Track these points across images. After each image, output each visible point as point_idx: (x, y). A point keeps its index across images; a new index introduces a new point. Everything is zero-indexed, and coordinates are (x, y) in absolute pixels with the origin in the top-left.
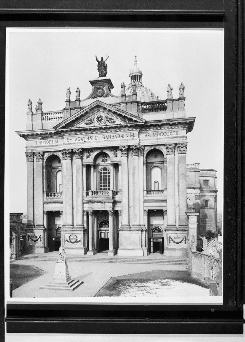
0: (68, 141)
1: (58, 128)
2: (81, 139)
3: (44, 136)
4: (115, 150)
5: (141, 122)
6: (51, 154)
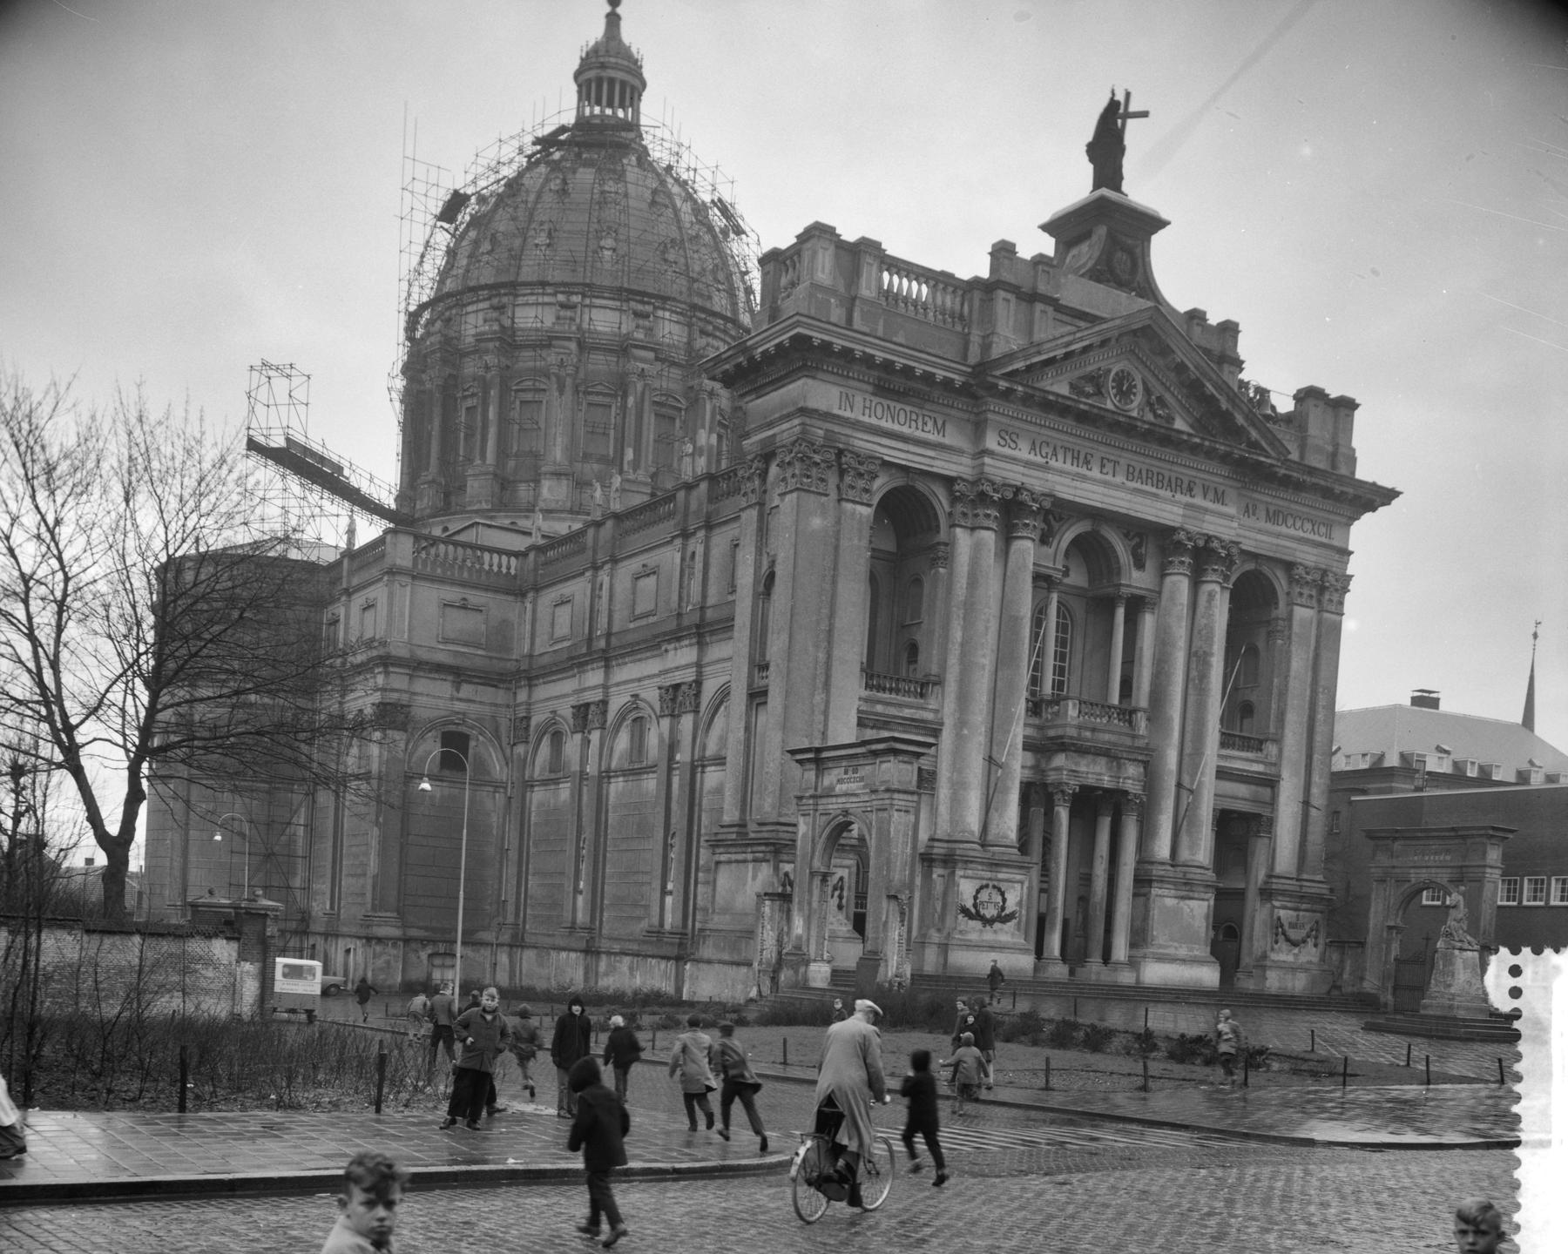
0: (1003, 442)
1: (998, 373)
2: (1050, 451)
4: (1137, 540)
5: (1273, 453)
6: (899, 481)
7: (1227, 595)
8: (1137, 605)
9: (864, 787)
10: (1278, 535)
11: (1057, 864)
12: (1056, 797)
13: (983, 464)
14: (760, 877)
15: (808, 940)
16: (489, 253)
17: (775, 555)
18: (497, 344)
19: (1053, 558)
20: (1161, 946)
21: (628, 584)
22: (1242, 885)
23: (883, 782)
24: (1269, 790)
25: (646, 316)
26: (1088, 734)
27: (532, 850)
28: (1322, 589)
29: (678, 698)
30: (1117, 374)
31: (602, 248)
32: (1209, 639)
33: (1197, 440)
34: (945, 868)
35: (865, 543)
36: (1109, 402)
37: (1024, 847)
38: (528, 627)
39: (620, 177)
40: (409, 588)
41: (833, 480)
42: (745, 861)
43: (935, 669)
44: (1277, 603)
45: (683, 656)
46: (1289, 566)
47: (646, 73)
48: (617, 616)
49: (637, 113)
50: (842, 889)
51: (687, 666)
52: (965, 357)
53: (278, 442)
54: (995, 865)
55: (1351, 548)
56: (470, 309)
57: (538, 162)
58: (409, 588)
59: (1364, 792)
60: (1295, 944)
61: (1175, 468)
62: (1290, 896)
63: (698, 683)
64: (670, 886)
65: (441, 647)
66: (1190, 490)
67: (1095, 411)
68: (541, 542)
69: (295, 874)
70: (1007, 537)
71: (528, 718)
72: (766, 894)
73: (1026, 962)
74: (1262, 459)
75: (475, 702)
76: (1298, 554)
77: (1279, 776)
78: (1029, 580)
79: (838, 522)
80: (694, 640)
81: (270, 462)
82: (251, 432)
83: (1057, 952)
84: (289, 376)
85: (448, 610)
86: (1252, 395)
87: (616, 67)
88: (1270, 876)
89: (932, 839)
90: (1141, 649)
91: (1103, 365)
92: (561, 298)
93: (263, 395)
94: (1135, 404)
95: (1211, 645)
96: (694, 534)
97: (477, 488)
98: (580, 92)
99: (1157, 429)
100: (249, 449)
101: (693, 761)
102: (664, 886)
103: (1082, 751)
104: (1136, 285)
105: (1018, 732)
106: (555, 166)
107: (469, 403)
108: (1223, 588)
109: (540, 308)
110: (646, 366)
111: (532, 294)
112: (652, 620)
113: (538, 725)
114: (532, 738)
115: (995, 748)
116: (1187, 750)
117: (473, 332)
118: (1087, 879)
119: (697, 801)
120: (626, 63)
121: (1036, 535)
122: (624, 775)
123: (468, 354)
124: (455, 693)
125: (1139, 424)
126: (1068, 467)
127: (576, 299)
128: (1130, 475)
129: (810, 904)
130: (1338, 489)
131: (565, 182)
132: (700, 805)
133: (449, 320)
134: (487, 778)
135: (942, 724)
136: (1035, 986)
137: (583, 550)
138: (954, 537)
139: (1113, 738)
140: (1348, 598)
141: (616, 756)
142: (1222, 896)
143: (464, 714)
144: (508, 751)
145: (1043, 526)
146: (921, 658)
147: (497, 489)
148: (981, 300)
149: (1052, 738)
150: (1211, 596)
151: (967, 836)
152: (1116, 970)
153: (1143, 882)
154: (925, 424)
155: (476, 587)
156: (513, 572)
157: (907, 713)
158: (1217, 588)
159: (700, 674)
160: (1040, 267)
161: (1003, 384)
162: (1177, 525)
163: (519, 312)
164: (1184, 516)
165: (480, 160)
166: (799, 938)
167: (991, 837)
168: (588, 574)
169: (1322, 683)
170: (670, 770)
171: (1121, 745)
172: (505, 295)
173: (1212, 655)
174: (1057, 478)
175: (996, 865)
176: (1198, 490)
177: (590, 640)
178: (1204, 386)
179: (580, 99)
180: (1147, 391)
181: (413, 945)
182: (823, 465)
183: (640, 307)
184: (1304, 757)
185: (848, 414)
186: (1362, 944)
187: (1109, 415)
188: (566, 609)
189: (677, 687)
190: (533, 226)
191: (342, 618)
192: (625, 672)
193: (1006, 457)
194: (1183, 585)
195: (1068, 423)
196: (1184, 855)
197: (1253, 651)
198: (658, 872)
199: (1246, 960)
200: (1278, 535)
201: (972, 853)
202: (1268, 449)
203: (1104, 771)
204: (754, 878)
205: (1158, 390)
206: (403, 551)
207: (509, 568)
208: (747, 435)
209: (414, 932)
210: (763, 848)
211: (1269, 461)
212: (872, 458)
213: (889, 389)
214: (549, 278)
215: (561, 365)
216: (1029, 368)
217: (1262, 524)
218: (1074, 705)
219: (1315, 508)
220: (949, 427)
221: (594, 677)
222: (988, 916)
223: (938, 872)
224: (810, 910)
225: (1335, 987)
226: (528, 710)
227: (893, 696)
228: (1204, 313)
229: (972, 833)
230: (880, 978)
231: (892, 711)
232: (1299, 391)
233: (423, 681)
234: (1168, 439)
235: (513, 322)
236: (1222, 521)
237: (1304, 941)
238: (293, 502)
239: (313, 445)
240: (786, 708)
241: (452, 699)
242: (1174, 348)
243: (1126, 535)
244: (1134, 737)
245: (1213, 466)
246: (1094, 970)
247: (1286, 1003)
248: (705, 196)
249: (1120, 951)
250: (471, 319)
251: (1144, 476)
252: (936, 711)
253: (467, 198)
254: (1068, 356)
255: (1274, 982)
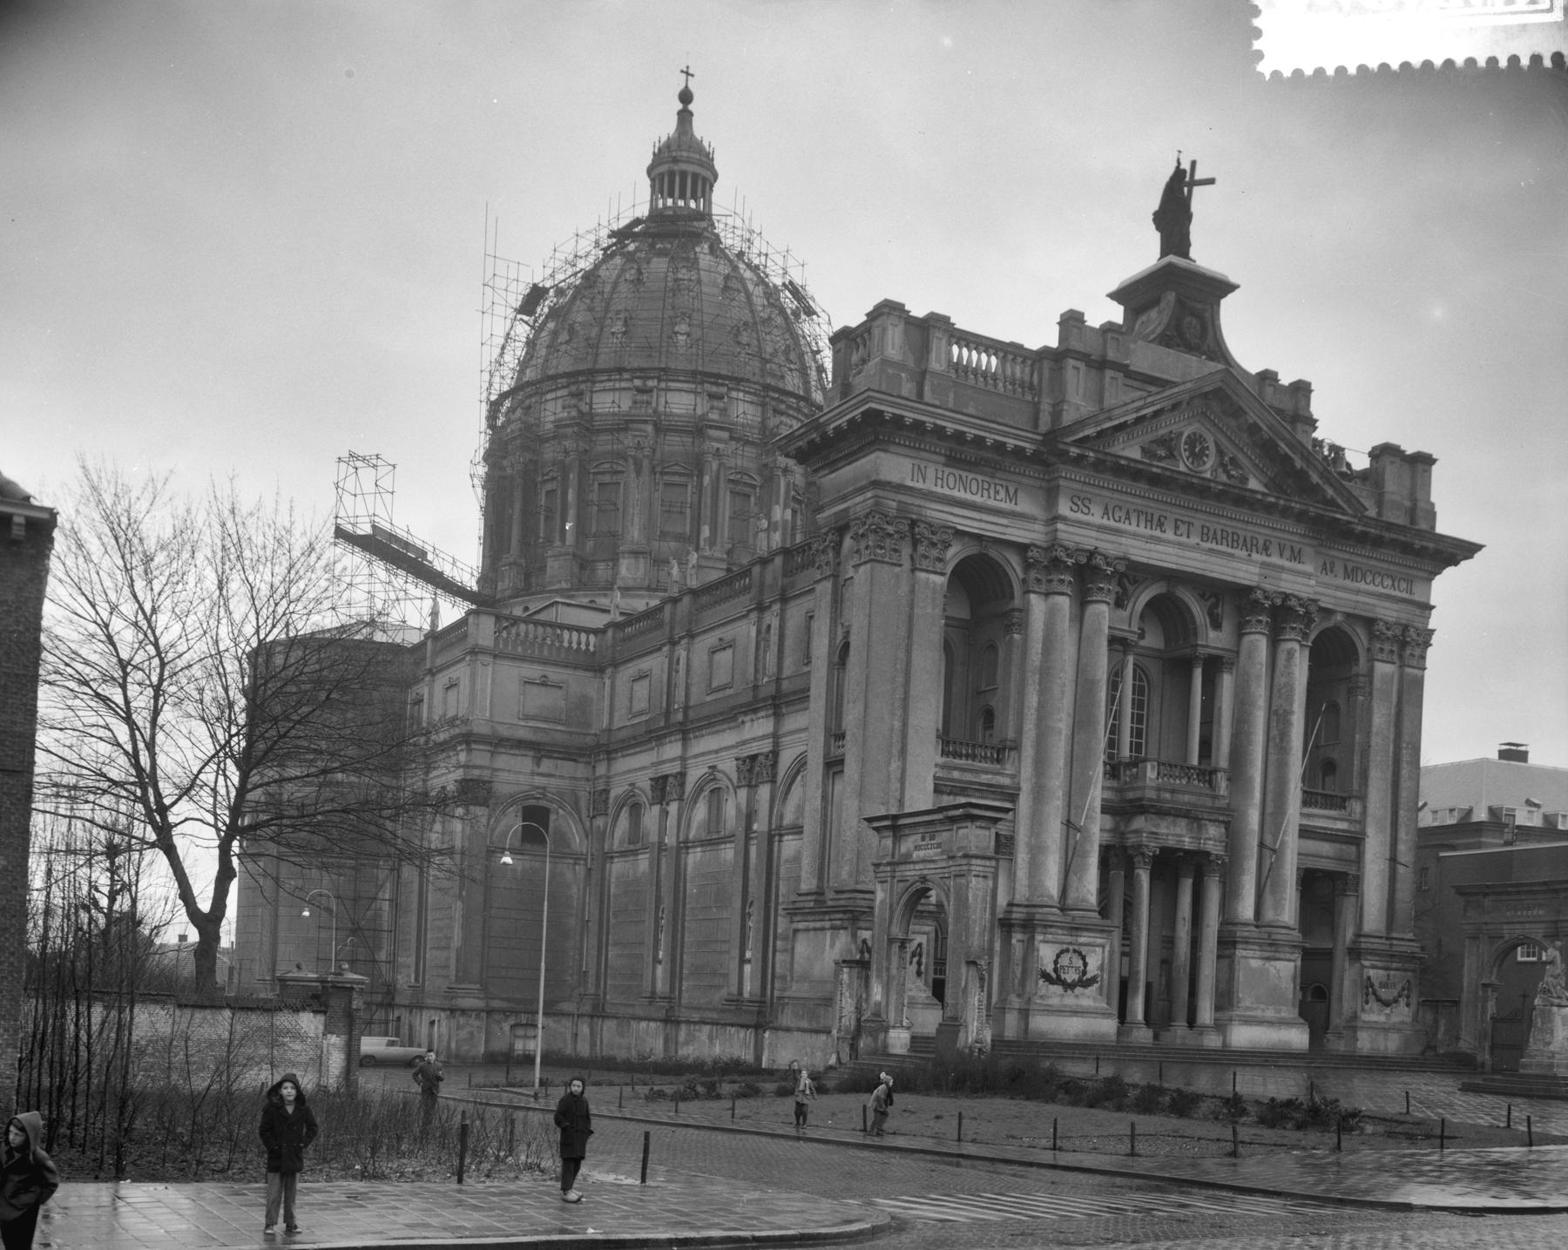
0: (1075, 508)
3: (971, 453)
4: (1213, 600)
5: (1350, 512)
6: (972, 549)
7: (1307, 652)
8: (1214, 666)
9: (942, 853)
10: (1358, 592)
11: (1139, 929)
12: (1136, 860)
13: (1056, 530)
14: (838, 945)
15: (887, 1005)
16: (567, 342)
17: (849, 626)
18: (576, 429)
19: (1128, 621)
20: (1247, 1009)
21: (706, 657)
22: (1330, 946)
23: (959, 849)
24: (1353, 848)
25: (720, 397)
26: (1167, 796)
27: (612, 921)
28: (1403, 644)
29: (756, 769)
30: (1189, 437)
31: (676, 333)
32: (1290, 699)
33: (1273, 500)
34: (1024, 933)
35: (938, 611)
36: (1181, 464)
37: (1104, 911)
38: (607, 703)
39: (694, 264)
40: (490, 668)
41: (906, 551)
42: (823, 929)
43: (1011, 735)
44: (1357, 660)
45: (762, 726)
46: (1369, 623)
47: (718, 165)
48: (694, 690)
49: (708, 203)
50: (920, 955)
51: (764, 737)
52: (1036, 425)
53: (365, 529)
54: (1075, 929)
55: (1432, 603)
56: (549, 396)
57: (613, 255)
58: (490, 668)
59: (1453, 848)
60: (1386, 1004)
61: (1250, 527)
62: (1379, 955)
63: (775, 753)
64: (748, 955)
65: (522, 723)
66: (1266, 548)
67: (1168, 473)
68: (620, 619)
69: (381, 948)
70: (1082, 601)
71: (607, 791)
72: (844, 961)
73: (1109, 1026)
74: (1338, 516)
75: (557, 776)
76: (1378, 610)
77: (1364, 834)
78: (1105, 643)
79: (912, 591)
80: (771, 712)
81: (357, 549)
82: (339, 521)
83: (1140, 1016)
84: (375, 466)
85: (528, 686)
86: (1326, 453)
87: (688, 161)
88: (1358, 935)
89: (1011, 904)
90: (1220, 708)
91: (1175, 428)
92: (638, 382)
93: (350, 485)
94: (1208, 465)
95: (1291, 704)
96: (770, 607)
97: (556, 568)
98: (653, 186)
99: (1232, 490)
100: (336, 537)
101: (770, 830)
102: (742, 954)
103: (1162, 812)
104: (1205, 348)
105: (1097, 793)
106: (630, 257)
107: (549, 487)
108: (1302, 646)
109: (617, 394)
110: (721, 446)
111: (610, 380)
112: (729, 692)
113: (617, 798)
114: (611, 811)
115: (1073, 812)
116: (1269, 810)
117: (552, 418)
118: (1170, 942)
119: (774, 870)
120: (698, 156)
121: (1111, 599)
122: (702, 846)
123: (547, 440)
124: (536, 769)
125: (1212, 485)
126: (1142, 530)
127: (651, 383)
128: (1205, 535)
129: (888, 969)
130: (1418, 543)
131: (639, 272)
132: (778, 874)
133: (529, 407)
134: (567, 851)
135: (1019, 789)
136: (1119, 1050)
137: (660, 625)
138: (1029, 602)
139: (1193, 799)
140: (1431, 653)
141: (694, 825)
142: (1308, 955)
143: (544, 788)
144: (588, 824)
145: (1118, 589)
146: (997, 723)
147: (576, 570)
148: (1052, 369)
149: (1131, 801)
150: (1290, 654)
151: (1046, 901)
152: (1201, 1034)
153: (1227, 943)
154: (997, 492)
155: (556, 664)
156: (591, 648)
157: (984, 778)
158: (1296, 646)
159: (776, 744)
160: (1110, 335)
161: (1074, 451)
162: (1254, 584)
163: (597, 398)
164: (1260, 575)
165: (557, 254)
166: (878, 1004)
167: (1070, 902)
168: (665, 649)
169: (1406, 738)
170: (748, 839)
171: (1201, 806)
172: (583, 382)
173: (1292, 713)
174: (1131, 542)
175: (1077, 929)
176: (1274, 549)
177: (668, 713)
178: (1277, 445)
179: (653, 193)
180: (1221, 453)
181: (497, 1017)
182: (896, 536)
183: (714, 389)
184: (1389, 816)
185: (920, 485)
186: (1456, 1003)
187: (1182, 477)
188: (645, 683)
189: (753, 758)
190: (609, 315)
191: (426, 697)
192: (706, 743)
193: (1079, 522)
194: (1262, 644)
195: (1140, 487)
196: (1269, 915)
197: (1334, 708)
198: (737, 943)
199: (1336, 1020)
200: (1358, 592)
201: (1052, 918)
202: (1345, 506)
203: (1184, 832)
204: (832, 945)
205: (1231, 451)
206: (485, 631)
207: (588, 645)
208: (820, 509)
209: (496, 1004)
210: (838, 916)
211: (1345, 518)
212: (946, 527)
213: (955, 458)
214: (626, 365)
215: (639, 447)
216: (1100, 434)
217: (1340, 581)
218: (1153, 768)
219: (1394, 563)
220: (1020, 494)
221: (672, 749)
222: (1069, 981)
223: (1017, 937)
224: (889, 977)
225: (1430, 1047)
226: (608, 783)
227: (970, 762)
228: (1276, 374)
229: (1051, 897)
230: (960, 1043)
231: (969, 777)
232: (1374, 448)
233: (504, 757)
234: (1243, 500)
235: (591, 408)
236: (1300, 579)
237: (1396, 1001)
238: (379, 587)
239: (398, 531)
240: (862, 776)
241: (533, 774)
242: (1247, 410)
243: (1202, 596)
244: (1215, 797)
245: (1290, 525)
246: (1179, 1033)
247: (1378, 1064)
248: (777, 281)
249: (1206, 1014)
250: (550, 406)
251: (1219, 537)
252: (1013, 777)
253: (545, 291)
254: (1139, 420)
255: (1365, 1043)
